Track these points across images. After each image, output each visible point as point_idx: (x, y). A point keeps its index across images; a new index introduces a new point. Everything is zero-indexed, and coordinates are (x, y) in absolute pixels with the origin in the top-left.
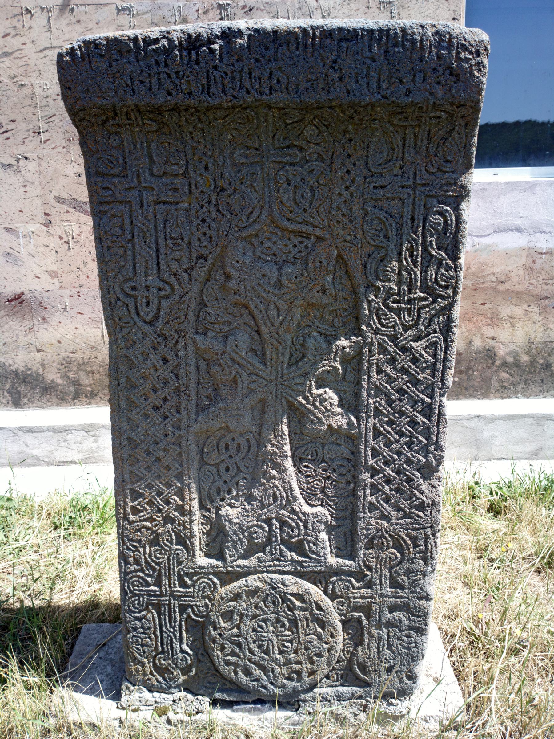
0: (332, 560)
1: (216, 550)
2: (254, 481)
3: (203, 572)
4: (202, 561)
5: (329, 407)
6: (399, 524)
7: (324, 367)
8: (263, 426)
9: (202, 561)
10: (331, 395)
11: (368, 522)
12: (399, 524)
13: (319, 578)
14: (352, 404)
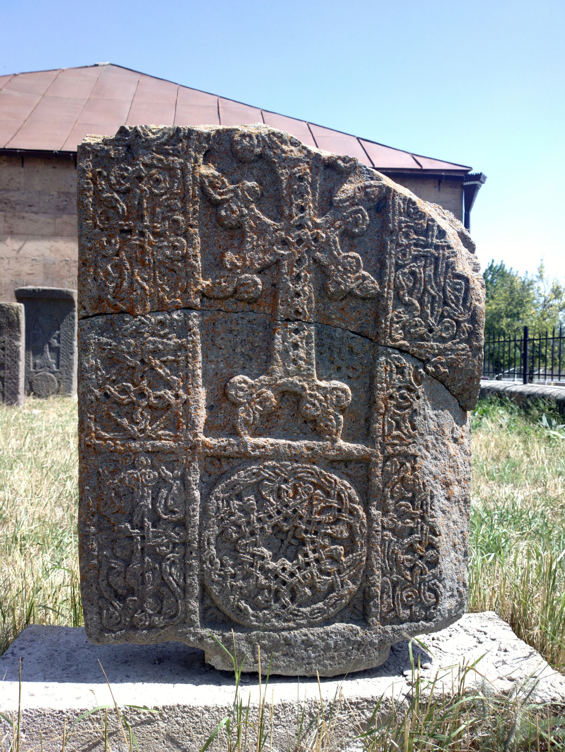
0: (55, 370)
1: (34, 368)
2: (42, 355)
3: (31, 372)
4: (32, 370)
5: (55, 342)
6: (67, 363)
7: (54, 336)
8: (44, 345)
9: (32, 370)
10: (55, 341)
11: (61, 363)
12: (67, 363)
13: (53, 373)
14: (59, 342)
